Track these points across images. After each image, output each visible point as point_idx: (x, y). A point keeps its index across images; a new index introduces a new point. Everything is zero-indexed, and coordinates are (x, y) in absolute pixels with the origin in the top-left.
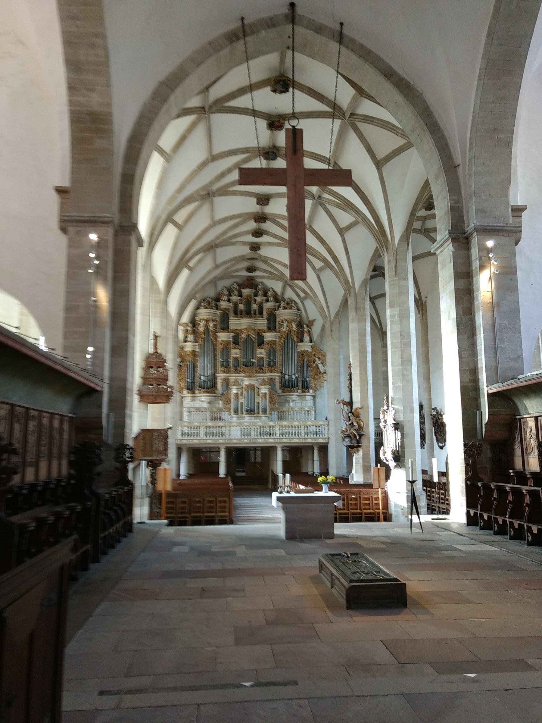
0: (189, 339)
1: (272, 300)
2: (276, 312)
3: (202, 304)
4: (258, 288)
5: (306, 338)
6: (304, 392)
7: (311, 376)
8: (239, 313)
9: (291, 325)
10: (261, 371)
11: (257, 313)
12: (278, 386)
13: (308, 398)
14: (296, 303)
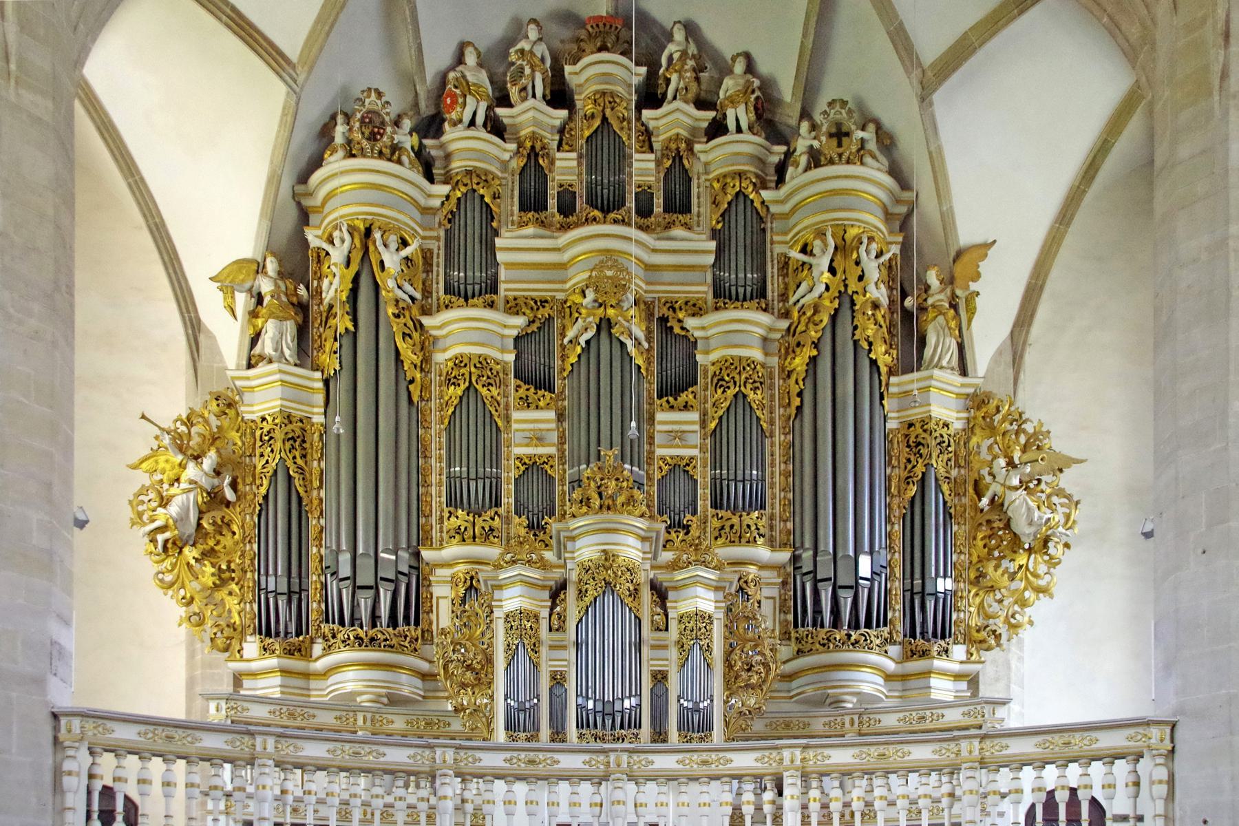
0: (267, 346)
1: (744, 125)
2: (766, 194)
4: (664, 61)
5: (940, 343)
6: (924, 654)
8: (552, 203)
11: (658, 208)
12: (768, 618)
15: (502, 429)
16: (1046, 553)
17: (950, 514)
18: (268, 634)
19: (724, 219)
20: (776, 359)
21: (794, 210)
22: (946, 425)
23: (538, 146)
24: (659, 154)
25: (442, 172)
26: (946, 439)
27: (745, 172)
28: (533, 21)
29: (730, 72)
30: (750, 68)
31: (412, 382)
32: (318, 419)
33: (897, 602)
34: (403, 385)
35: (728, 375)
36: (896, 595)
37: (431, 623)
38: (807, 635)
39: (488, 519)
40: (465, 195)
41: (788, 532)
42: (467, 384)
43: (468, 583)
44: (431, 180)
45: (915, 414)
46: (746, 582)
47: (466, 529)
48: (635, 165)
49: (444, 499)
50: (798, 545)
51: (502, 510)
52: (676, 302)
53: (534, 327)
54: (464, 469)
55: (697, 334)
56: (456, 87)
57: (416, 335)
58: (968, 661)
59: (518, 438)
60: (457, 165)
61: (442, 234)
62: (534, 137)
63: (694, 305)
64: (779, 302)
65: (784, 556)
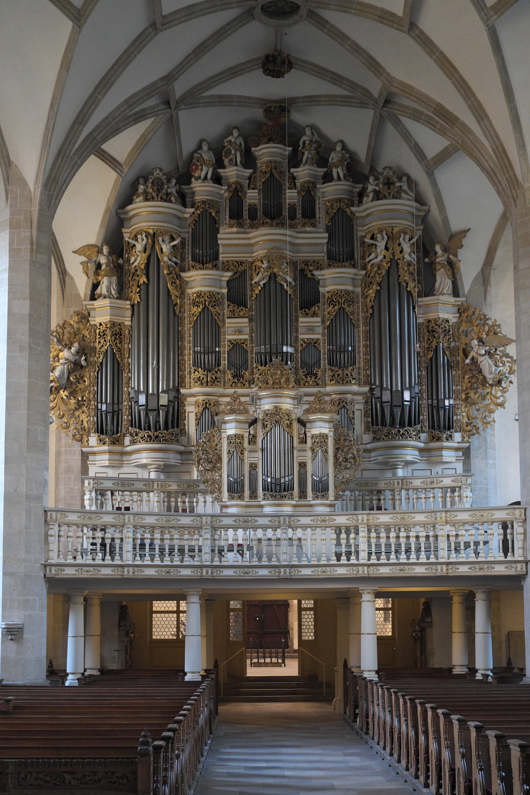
0: (103, 289)
2: (353, 209)
3: (141, 188)
4: (301, 144)
6: (439, 439)
7: (458, 392)
8: (246, 214)
9: (399, 245)
10: (311, 381)
11: (299, 216)
13: (448, 456)
14: (410, 181)
15: (221, 326)
16: (501, 386)
17: (451, 366)
18: (102, 433)
19: (332, 221)
20: (360, 289)
21: (367, 216)
22: (448, 321)
23: (238, 186)
24: (299, 188)
25: (190, 200)
26: (447, 328)
27: (343, 198)
28: (236, 127)
29: (334, 149)
30: (344, 147)
31: (176, 304)
32: (128, 323)
33: (424, 411)
34: (171, 307)
35: (335, 299)
36: (424, 407)
37: (185, 425)
38: (378, 431)
39: (214, 373)
40: (202, 212)
41: (368, 376)
42: (204, 306)
43: (204, 405)
44: (185, 206)
45: (432, 316)
46: (346, 403)
47: (203, 378)
48: (287, 194)
49: (191, 362)
50: (373, 382)
51: (221, 368)
52: (309, 262)
53: (237, 276)
54: (202, 348)
55: (319, 277)
56: (198, 161)
57: (178, 282)
58: (463, 442)
59: (230, 330)
60: (198, 198)
61: (190, 230)
62: (237, 183)
63: (318, 263)
64: (361, 260)
65: (366, 389)
